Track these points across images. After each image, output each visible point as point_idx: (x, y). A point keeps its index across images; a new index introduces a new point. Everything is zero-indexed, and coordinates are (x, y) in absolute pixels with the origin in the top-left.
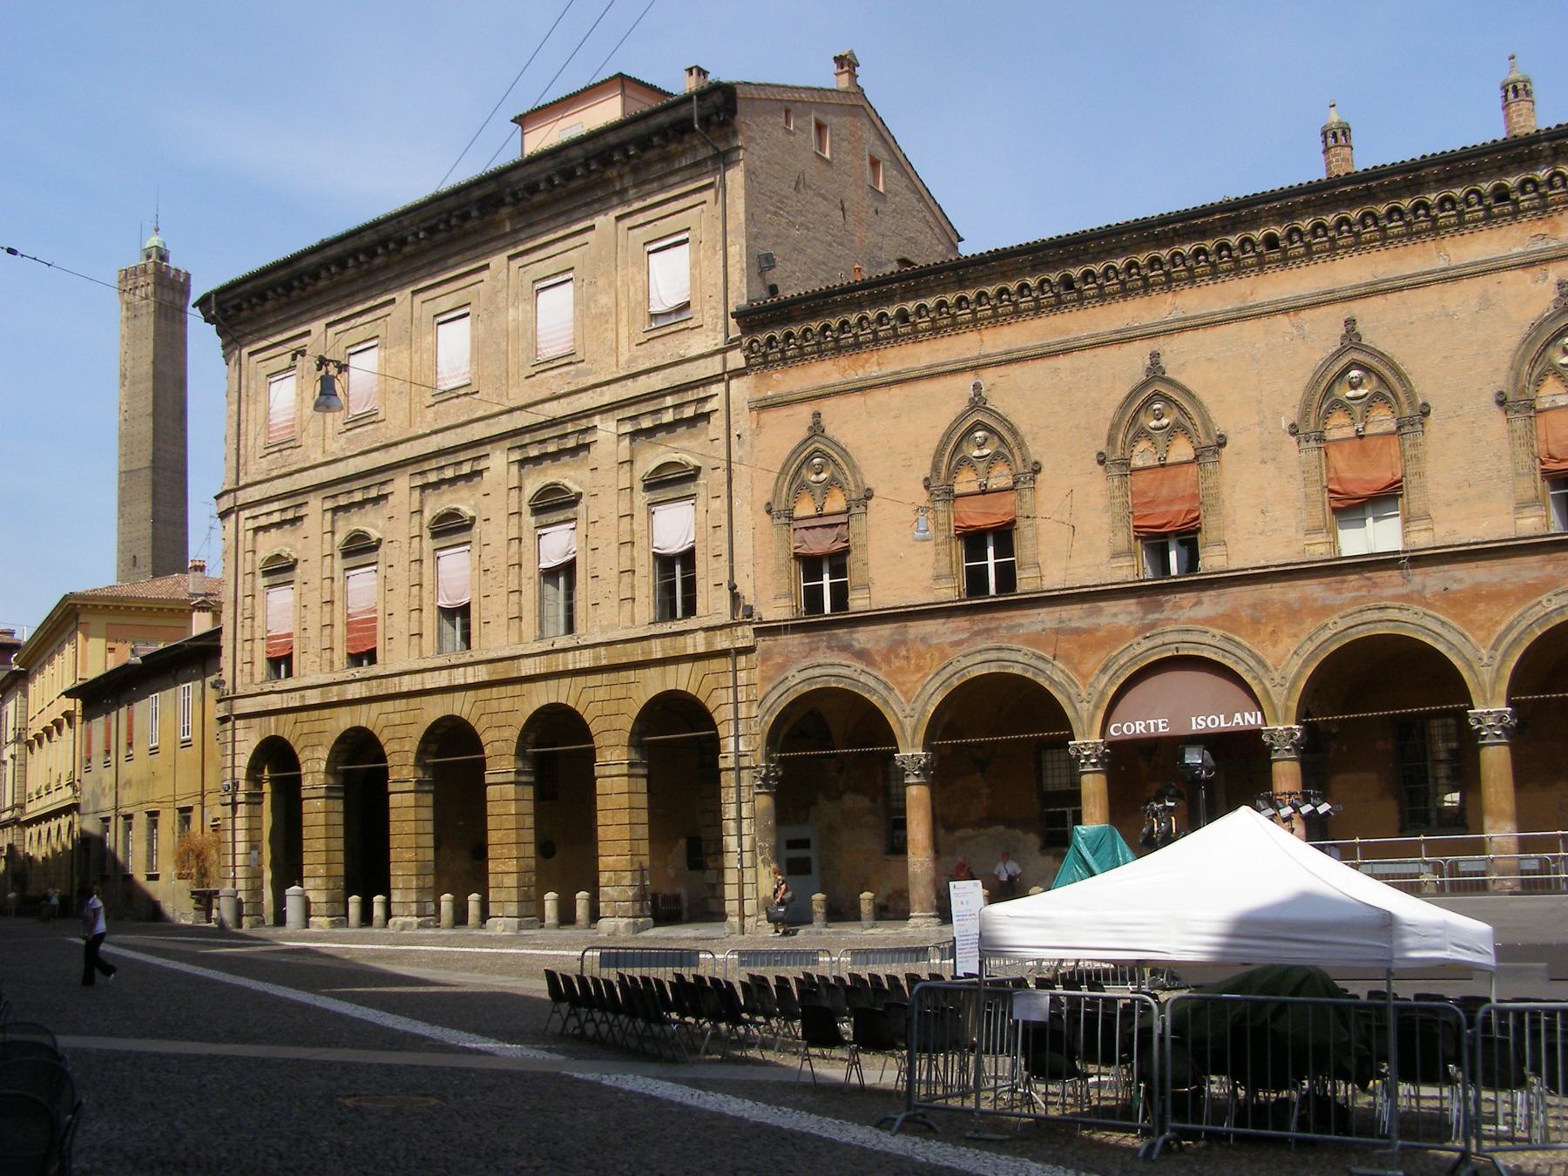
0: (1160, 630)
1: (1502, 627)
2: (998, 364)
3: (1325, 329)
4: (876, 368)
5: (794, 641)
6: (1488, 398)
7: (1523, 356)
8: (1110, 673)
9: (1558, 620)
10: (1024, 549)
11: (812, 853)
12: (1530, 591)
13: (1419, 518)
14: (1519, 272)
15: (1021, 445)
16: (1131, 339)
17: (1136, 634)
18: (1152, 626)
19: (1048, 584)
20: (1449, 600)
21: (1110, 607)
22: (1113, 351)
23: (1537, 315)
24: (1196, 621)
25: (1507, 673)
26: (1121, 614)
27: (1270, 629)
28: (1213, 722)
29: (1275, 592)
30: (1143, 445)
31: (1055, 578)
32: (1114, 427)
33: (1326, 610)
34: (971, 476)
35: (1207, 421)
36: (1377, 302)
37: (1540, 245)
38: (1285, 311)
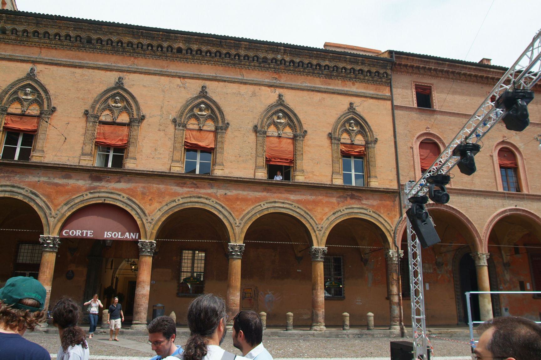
0: (98, 190)
1: (246, 212)
2: (46, 63)
3: (194, 87)
6: (251, 127)
7: (265, 116)
8: (69, 206)
9: (266, 212)
10: (39, 143)
12: (258, 200)
13: (220, 165)
14: (267, 88)
15: (49, 99)
16: (111, 70)
17: (86, 191)
18: (95, 188)
19: (46, 161)
22: (102, 73)
23: (271, 103)
24: (116, 189)
25: (245, 230)
27: (150, 198)
28: (115, 235)
30: (107, 112)
31: (50, 158)
32: (96, 102)
33: (176, 194)
34: (19, 106)
35: (138, 109)
36: (216, 83)
37: (274, 81)
38: (179, 77)
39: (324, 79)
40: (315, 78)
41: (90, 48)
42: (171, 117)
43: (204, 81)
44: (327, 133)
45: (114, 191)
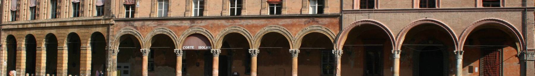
5: (122, 23)
11: (129, 69)
20: (248, 27)
21: (185, 22)
26: (187, 23)
29: (216, 22)
33: (224, 27)
45: (200, 27)
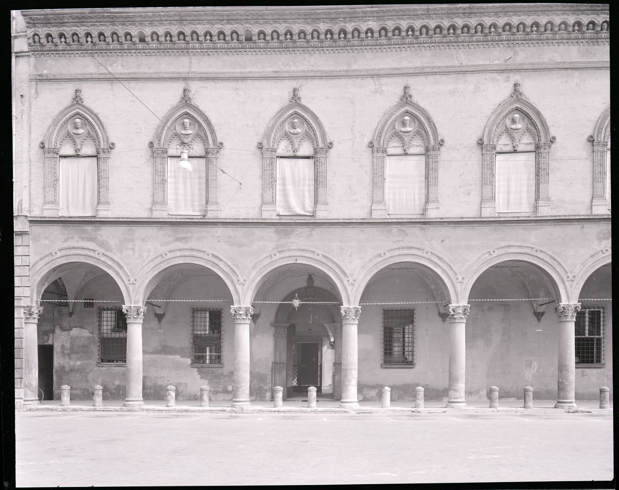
2: (201, 79)
4: (120, 68)
7: (494, 121)
15: (213, 131)
16: (283, 78)
32: (270, 129)
35: (324, 135)
38: (372, 76)
39: (586, 47)
40: (572, 47)
41: (251, 48)
42: (366, 141)
43: (406, 78)
44: (586, 137)
